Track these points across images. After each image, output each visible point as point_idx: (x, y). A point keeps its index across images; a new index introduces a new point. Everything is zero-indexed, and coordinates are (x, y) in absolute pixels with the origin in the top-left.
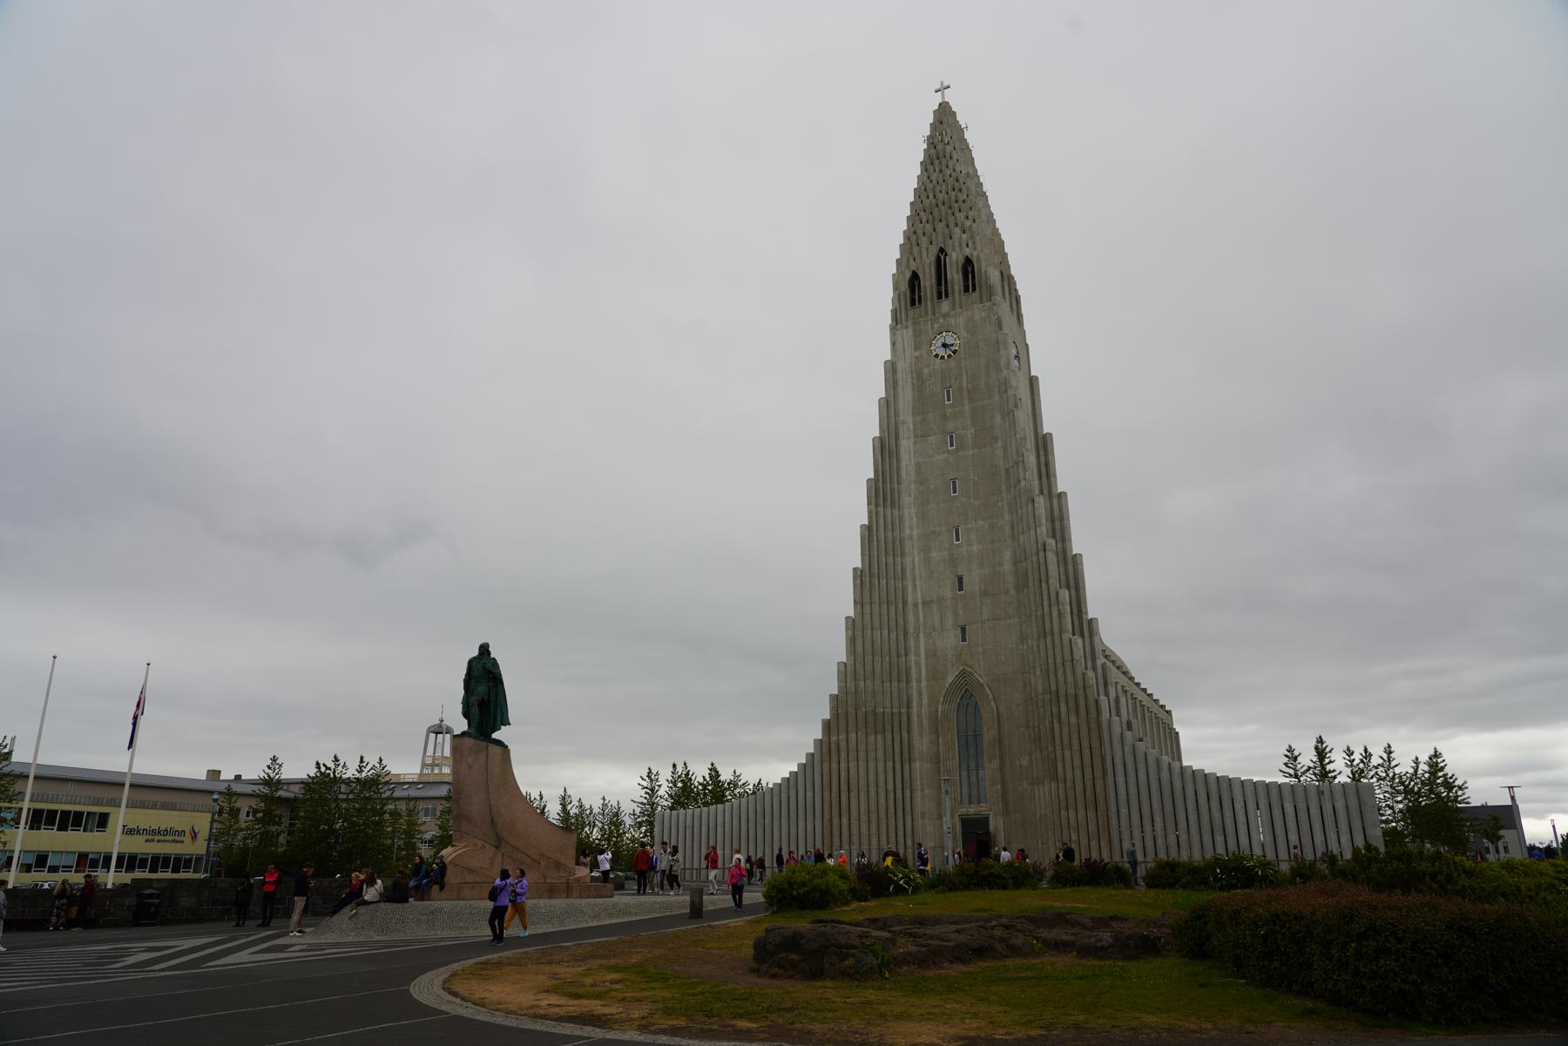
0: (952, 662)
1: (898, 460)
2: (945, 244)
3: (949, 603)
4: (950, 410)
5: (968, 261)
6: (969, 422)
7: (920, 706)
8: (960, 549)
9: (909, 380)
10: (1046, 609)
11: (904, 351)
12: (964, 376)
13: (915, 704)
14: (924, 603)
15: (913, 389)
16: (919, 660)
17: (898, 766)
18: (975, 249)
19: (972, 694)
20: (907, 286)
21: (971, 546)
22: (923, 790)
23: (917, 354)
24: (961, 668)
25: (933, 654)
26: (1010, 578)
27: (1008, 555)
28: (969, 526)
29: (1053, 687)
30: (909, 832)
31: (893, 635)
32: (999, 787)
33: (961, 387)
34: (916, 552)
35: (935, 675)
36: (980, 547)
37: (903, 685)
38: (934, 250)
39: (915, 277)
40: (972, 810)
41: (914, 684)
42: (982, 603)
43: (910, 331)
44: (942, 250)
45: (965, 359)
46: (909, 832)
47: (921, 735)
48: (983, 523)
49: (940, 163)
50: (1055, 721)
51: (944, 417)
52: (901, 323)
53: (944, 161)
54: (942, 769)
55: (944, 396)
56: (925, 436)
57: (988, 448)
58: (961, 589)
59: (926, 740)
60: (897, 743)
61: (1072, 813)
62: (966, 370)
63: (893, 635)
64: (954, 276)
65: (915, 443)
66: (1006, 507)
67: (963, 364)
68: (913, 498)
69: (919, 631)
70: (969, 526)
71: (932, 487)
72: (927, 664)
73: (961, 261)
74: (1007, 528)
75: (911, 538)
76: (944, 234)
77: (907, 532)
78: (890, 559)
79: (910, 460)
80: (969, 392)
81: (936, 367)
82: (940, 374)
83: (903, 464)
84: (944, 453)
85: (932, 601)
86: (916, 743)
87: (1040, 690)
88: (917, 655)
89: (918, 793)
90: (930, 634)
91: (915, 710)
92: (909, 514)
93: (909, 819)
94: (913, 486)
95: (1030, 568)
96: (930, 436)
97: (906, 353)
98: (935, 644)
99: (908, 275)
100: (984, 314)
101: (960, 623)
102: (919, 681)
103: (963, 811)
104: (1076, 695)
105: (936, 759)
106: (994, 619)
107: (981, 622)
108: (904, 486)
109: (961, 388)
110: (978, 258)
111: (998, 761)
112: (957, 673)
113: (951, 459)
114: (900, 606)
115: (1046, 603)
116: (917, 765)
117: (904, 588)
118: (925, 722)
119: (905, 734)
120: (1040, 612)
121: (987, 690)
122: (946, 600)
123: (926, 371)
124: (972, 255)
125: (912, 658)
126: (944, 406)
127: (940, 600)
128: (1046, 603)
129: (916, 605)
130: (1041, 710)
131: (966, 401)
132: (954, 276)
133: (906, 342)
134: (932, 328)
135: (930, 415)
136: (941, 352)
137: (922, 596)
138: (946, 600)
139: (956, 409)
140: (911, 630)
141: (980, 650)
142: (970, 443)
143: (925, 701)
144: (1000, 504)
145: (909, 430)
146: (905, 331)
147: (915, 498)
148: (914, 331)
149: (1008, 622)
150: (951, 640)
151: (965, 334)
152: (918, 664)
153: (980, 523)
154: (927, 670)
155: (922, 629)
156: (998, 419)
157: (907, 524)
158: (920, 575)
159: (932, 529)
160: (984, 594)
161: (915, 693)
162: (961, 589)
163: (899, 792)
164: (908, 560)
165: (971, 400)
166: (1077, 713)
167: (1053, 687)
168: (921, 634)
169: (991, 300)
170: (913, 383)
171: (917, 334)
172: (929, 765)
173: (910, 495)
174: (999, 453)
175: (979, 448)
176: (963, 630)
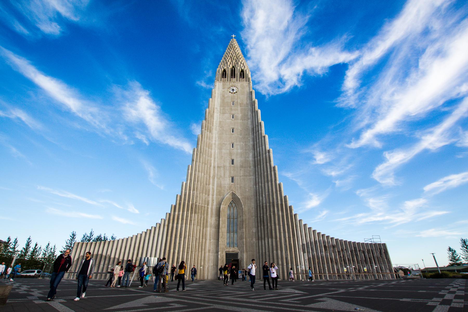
0: (227, 190)
1: (213, 119)
2: (234, 66)
3: (228, 168)
4: (233, 108)
6: (239, 112)
7: (212, 205)
8: (233, 151)
9: (220, 97)
10: (269, 172)
11: (219, 89)
12: (239, 99)
13: (210, 204)
14: (218, 167)
15: (221, 99)
16: (214, 187)
17: (202, 228)
18: (245, 67)
19: (234, 202)
20: (222, 72)
21: (238, 150)
22: (210, 240)
23: (224, 90)
24: (232, 192)
25: (220, 186)
27: (251, 155)
28: (237, 143)
29: (271, 201)
30: (203, 258)
31: (205, 176)
32: (244, 240)
33: (238, 102)
34: (216, 149)
35: (219, 193)
36: (241, 151)
37: (207, 196)
38: (231, 66)
39: (225, 71)
40: (231, 250)
41: (211, 196)
42: (240, 170)
43: (222, 84)
44: (233, 67)
45: (240, 95)
46: (203, 258)
47: (212, 217)
48: (242, 143)
49: (234, 49)
50: (272, 214)
51: (231, 109)
52: (219, 81)
53: (235, 49)
54: (220, 231)
55: (231, 103)
56: (224, 113)
57: (246, 121)
58: (233, 163)
60: (202, 219)
62: (240, 98)
63: (205, 176)
65: (220, 115)
66: (251, 140)
67: (239, 96)
68: (217, 132)
69: (215, 177)
70: (237, 143)
71: (225, 129)
72: (217, 189)
73: (240, 70)
74: (251, 146)
75: (215, 144)
76: (235, 63)
77: (214, 142)
78: (207, 149)
79: (217, 119)
80: (240, 104)
81: (229, 95)
82: (231, 97)
83: (215, 120)
84: (230, 119)
85: (221, 167)
86: (209, 220)
87: (264, 202)
88: (213, 185)
89: (208, 241)
90: (219, 178)
91: (210, 207)
92: (215, 136)
93: (203, 252)
94: (217, 128)
95: (261, 158)
96: (226, 114)
97: (220, 89)
98: (221, 182)
100: (247, 84)
102: (213, 195)
103: (228, 250)
105: (218, 227)
106: (245, 176)
107: (240, 176)
108: (214, 127)
109: (238, 102)
110: (246, 70)
111: (244, 229)
112: (230, 193)
113: (232, 122)
114: (209, 166)
115: (269, 170)
116: (209, 229)
117: (211, 160)
119: (205, 215)
120: (265, 174)
121: (241, 201)
122: (227, 167)
123: (226, 95)
124: (244, 69)
125: (211, 186)
126: (231, 106)
127: (224, 167)
128: (269, 170)
130: (265, 210)
131: (239, 106)
132: (238, 73)
133: (220, 87)
134: (229, 84)
135: (226, 108)
136: (232, 91)
137: (218, 164)
138: (227, 167)
139: (236, 108)
140: (212, 176)
141: (239, 186)
142: (240, 118)
143: (215, 203)
144: (249, 138)
145: (218, 111)
146: (220, 83)
147: (218, 132)
148: (223, 84)
149: (250, 177)
150: (228, 181)
151: (240, 88)
152: (213, 189)
153: (242, 143)
154: (217, 192)
155: (216, 176)
157: (214, 139)
158: (217, 157)
159: (223, 142)
160: (242, 167)
161: (210, 199)
162: (233, 163)
163: (201, 240)
164: (213, 151)
165: (240, 106)
167: (271, 201)
168: (216, 178)
169: (249, 81)
170: (221, 98)
172: (214, 229)
173: (216, 130)
175: (243, 120)
176: (233, 179)
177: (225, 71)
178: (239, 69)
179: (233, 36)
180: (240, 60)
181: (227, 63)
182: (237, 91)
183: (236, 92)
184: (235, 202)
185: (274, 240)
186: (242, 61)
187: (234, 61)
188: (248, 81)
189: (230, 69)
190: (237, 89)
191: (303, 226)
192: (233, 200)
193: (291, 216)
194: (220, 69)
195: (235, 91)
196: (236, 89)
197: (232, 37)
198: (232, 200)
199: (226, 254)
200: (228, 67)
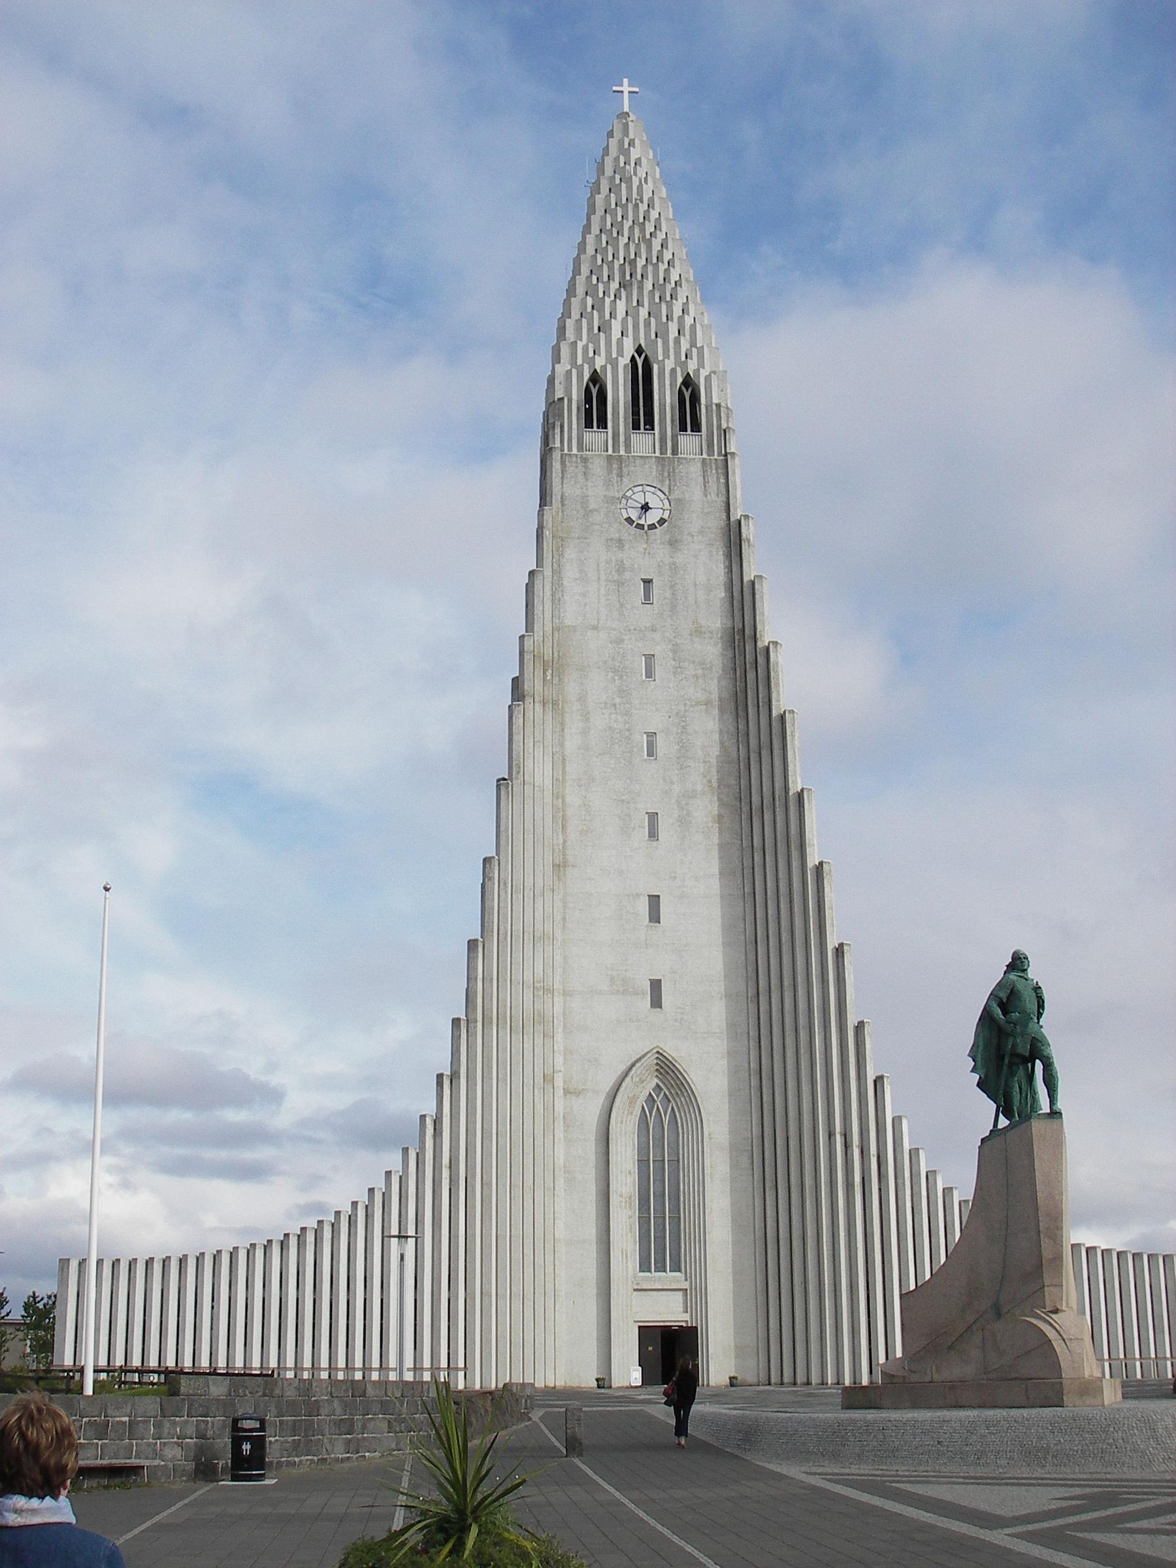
5: (688, 382)
18: (701, 364)
19: (665, 1093)
39: (595, 378)
44: (639, 350)
76: (647, 324)
99: (587, 376)
124: (698, 370)
132: (665, 397)
177: (595, 378)
178: (673, 371)
179: (626, 88)
180: (677, 311)
181: (604, 328)
182: (666, 516)
183: (662, 521)
184: (667, 1093)
187: (643, 313)
188: (720, 454)
189: (625, 366)
190: (666, 502)
191: (940, 1194)
192: (661, 1085)
194: (574, 371)
195: (652, 517)
196: (662, 506)
197: (615, 91)
198: (658, 1085)
200: (614, 356)
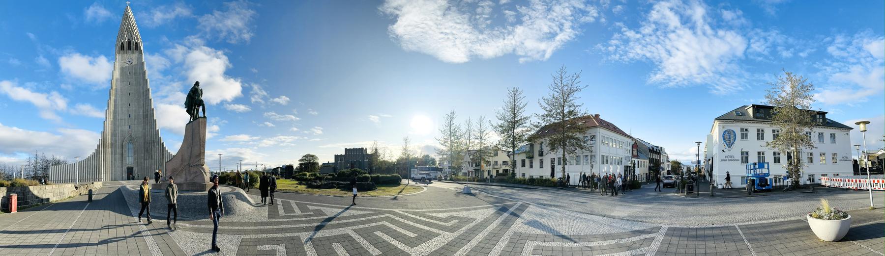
7: (118, 142)
25: (122, 131)
26: (142, 116)
39: (122, 43)
50: (153, 147)
58: (130, 117)
59: (120, 150)
61: (155, 166)
64: (133, 46)
75: (118, 104)
88: (118, 131)
101: (130, 124)
102: (118, 137)
104: (158, 142)
118: (120, 145)
129: (119, 120)
136: (128, 63)
143: (120, 141)
150: (127, 128)
152: (118, 133)
156: (142, 80)
162: (130, 117)
166: (158, 145)
171: (122, 57)
174: (141, 88)
177: (122, 43)
185: (153, 160)
186: (136, 33)
193: (163, 148)
199: (127, 168)
